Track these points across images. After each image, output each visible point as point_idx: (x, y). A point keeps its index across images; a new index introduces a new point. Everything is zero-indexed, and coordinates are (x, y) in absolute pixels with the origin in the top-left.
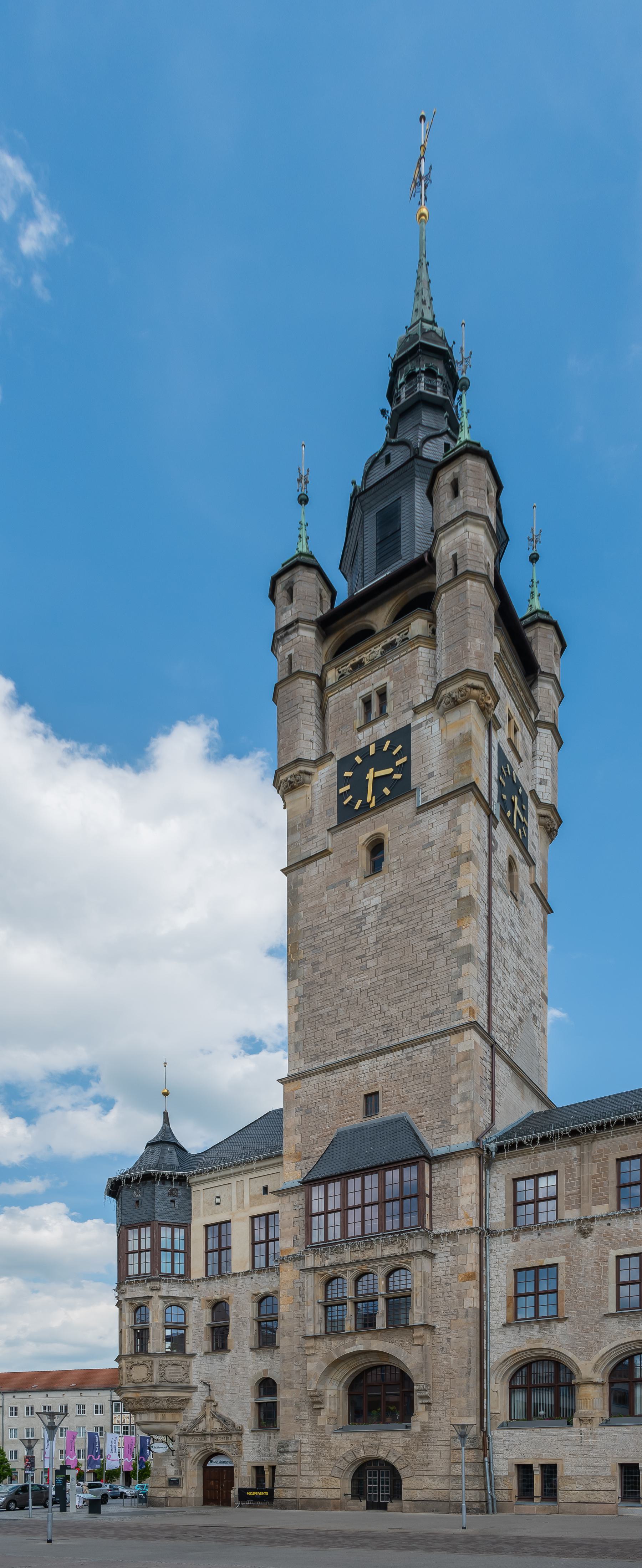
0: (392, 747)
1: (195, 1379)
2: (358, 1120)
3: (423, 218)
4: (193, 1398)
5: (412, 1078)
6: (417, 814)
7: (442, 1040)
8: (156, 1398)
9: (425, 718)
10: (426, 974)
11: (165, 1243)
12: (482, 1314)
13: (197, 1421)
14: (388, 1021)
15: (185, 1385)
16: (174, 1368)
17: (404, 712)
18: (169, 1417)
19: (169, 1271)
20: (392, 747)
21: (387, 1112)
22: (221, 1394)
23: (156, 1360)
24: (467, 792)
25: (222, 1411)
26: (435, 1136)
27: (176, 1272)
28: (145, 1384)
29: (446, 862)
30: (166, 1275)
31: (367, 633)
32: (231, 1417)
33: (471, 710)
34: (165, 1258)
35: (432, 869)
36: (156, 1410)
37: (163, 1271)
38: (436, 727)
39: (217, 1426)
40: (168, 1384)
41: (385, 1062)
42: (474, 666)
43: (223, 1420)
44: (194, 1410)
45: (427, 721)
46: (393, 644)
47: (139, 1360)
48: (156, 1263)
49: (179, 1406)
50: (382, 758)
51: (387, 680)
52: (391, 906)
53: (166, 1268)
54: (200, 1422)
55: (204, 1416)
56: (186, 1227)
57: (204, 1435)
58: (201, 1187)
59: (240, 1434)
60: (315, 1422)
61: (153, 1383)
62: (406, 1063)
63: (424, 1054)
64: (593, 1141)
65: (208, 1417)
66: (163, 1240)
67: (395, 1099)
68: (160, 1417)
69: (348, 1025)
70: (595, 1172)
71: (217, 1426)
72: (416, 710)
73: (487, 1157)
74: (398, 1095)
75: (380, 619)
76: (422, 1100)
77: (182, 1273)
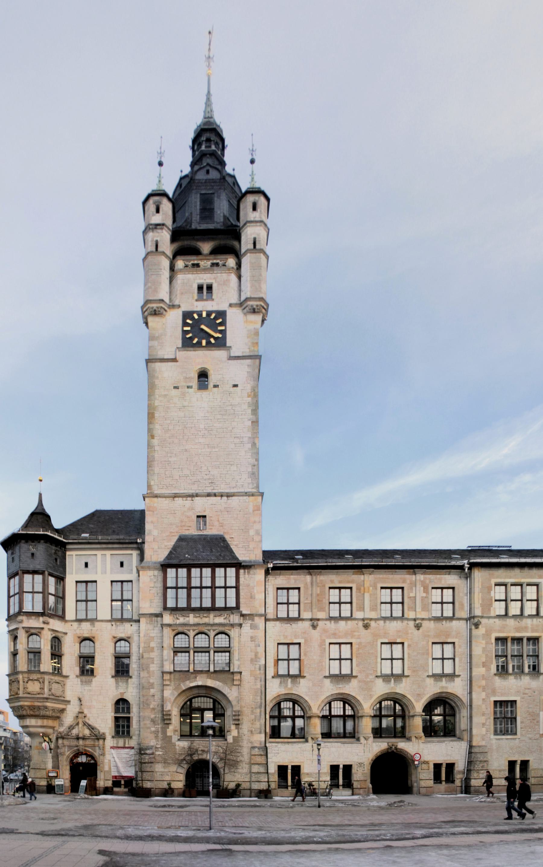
0: (216, 318)
1: (69, 695)
2: (192, 531)
4: (67, 709)
5: (226, 513)
13: (71, 728)
15: (62, 699)
18: (50, 723)
20: (216, 318)
21: (212, 530)
25: (91, 722)
26: (241, 552)
28: (38, 696)
31: (197, 252)
36: (44, 717)
39: (87, 732)
43: (91, 728)
46: (217, 265)
49: (58, 715)
51: (213, 281)
54: (73, 728)
55: (78, 724)
56: (61, 579)
57: (78, 738)
58: (74, 553)
59: (104, 739)
65: (80, 725)
67: (216, 523)
68: (46, 722)
71: (87, 732)
72: (231, 305)
74: (218, 521)
75: (206, 247)
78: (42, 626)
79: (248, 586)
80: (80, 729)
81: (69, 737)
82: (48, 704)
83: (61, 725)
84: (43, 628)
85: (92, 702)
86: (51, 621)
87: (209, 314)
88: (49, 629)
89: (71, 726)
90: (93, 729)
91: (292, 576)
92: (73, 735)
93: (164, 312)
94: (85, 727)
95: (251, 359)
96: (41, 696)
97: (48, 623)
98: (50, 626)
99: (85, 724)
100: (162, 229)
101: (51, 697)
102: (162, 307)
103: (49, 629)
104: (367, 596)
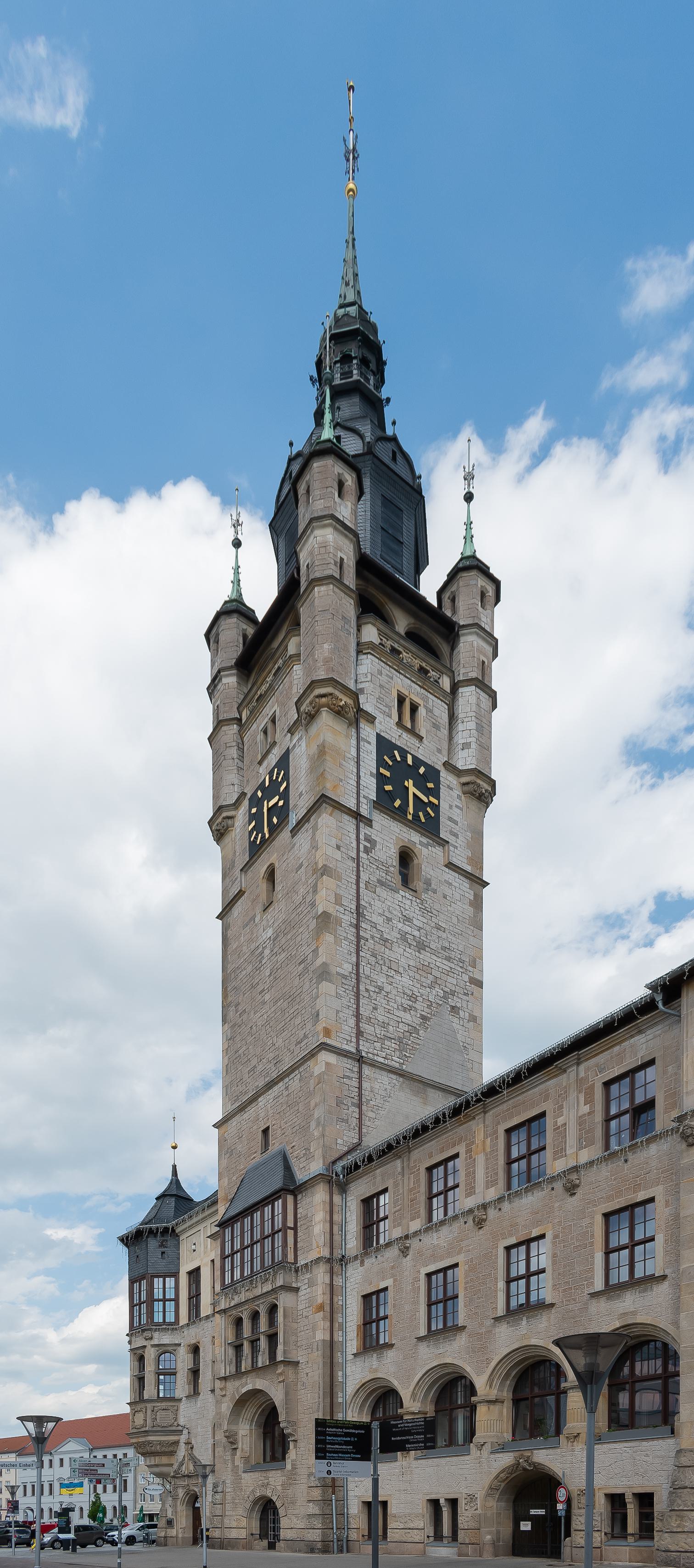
3: (351, 193)
6: (293, 837)
7: (305, 1066)
8: (149, 1442)
9: (297, 738)
10: (298, 1000)
11: (158, 1294)
12: (331, 1347)
14: (277, 1053)
16: (164, 1413)
17: (285, 735)
19: (161, 1320)
23: (149, 1406)
24: (321, 805)
27: (167, 1320)
29: (310, 882)
30: (158, 1324)
33: (325, 718)
34: (158, 1307)
35: (302, 891)
37: (156, 1320)
38: (303, 744)
40: (159, 1429)
41: (273, 1095)
42: (322, 675)
45: (300, 739)
47: (138, 1408)
48: (151, 1313)
50: (270, 790)
52: (278, 936)
53: (158, 1318)
56: (175, 1275)
60: (233, 1461)
61: (147, 1429)
62: (285, 1093)
63: (294, 1082)
64: (410, 1152)
66: (156, 1291)
69: (254, 1062)
70: (412, 1185)
73: (339, 1179)
76: (295, 1130)
77: (173, 1320)
78: (145, 1343)
79: (306, 1216)
82: (151, 1438)
84: (145, 1347)
86: (156, 1335)
87: (271, 773)
88: (153, 1346)
91: (378, 1171)
93: (230, 822)
95: (315, 812)
96: (143, 1430)
97: (151, 1338)
98: (155, 1342)
100: (220, 680)
101: (155, 1429)
102: (224, 818)
103: (153, 1346)
104: (480, 1160)
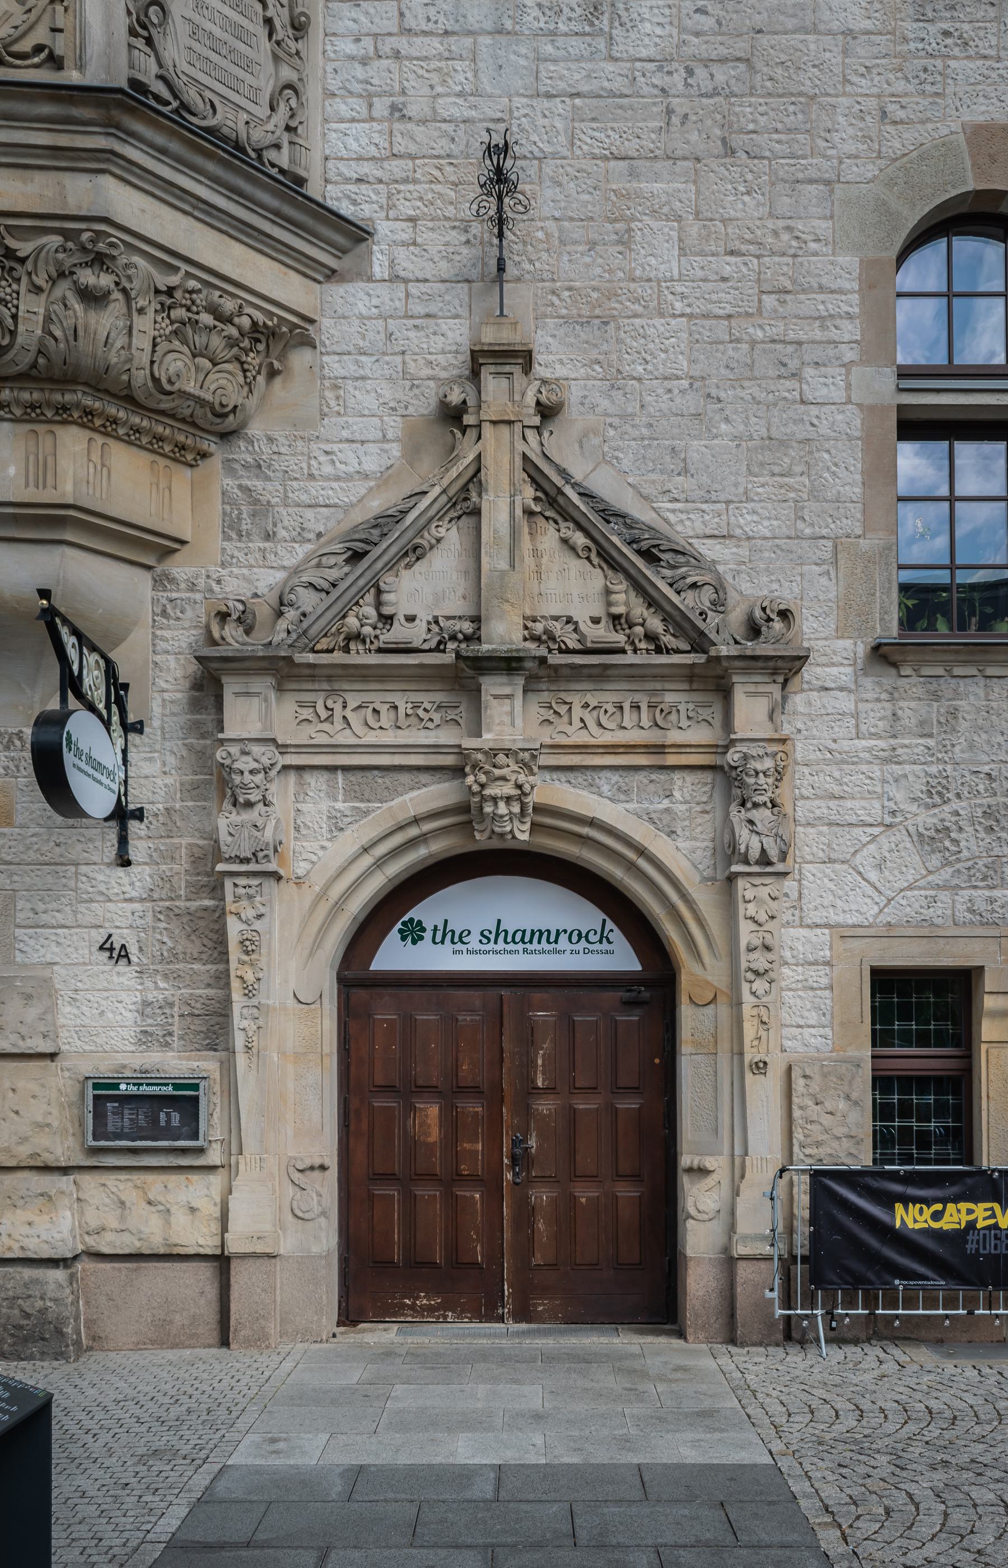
18: (122, 479)
22: (595, 319)
32: (682, 524)
39: (570, 591)
44: (339, 439)
49: (223, 385)
80: (494, 561)
81: (360, 657)
83: (251, 520)
85: (625, 241)
89: (386, 522)
90: (649, 556)
92: (399, 633)
94: (549, 537)
99: (549, 498)
